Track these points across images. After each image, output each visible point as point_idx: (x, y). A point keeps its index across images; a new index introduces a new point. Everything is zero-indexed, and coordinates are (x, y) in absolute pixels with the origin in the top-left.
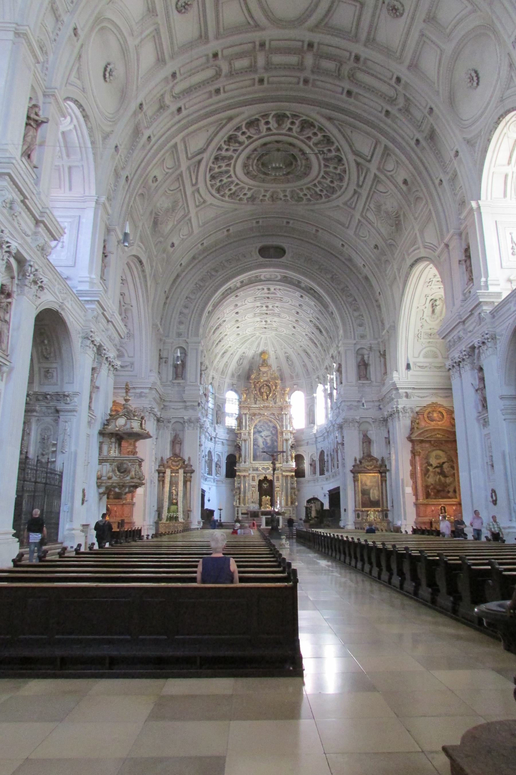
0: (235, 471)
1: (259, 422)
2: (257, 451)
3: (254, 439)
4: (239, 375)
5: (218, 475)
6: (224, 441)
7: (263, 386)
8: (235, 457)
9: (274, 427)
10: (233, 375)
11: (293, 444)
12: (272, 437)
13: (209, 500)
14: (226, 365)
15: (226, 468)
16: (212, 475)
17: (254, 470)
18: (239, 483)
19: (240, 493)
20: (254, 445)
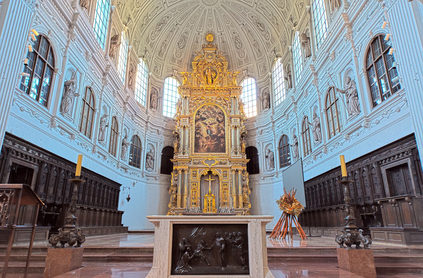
0: (172, 164)
1: (203, 108)
2: (200, 141)
3: (196, 127)
4: (181, 61)
5: (148, 169)
6: (160, 130)
7: (208, 69)
8: (173, 149)
9: (220, 113)
10: (173, 60)
11: (244, 133)
12: (219, 125)
13: (128, 199)
14: (164, 44)
15: (161, 162)
16: (139, 167)
17: (195, 163)
18: (176, 180)
19: (177, 192)
20: (196, 133)
